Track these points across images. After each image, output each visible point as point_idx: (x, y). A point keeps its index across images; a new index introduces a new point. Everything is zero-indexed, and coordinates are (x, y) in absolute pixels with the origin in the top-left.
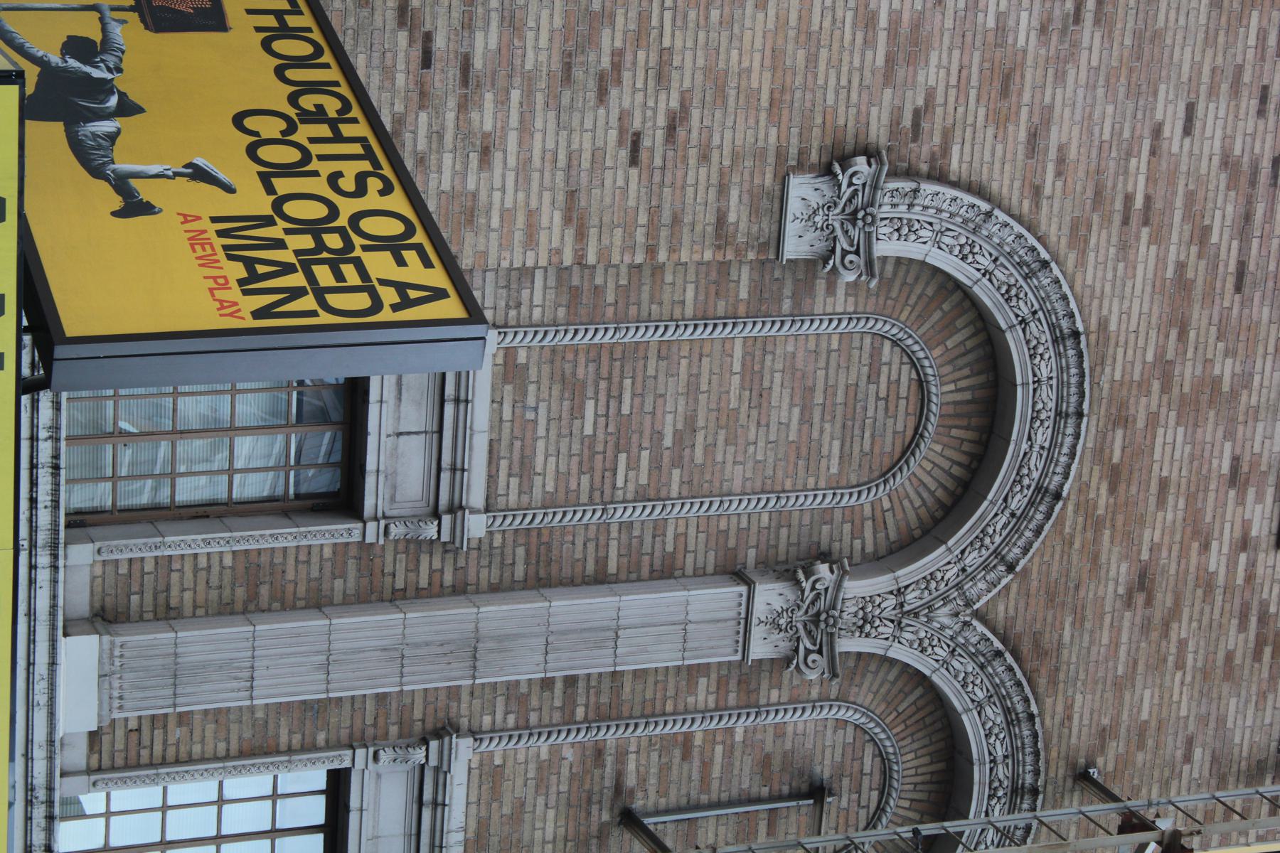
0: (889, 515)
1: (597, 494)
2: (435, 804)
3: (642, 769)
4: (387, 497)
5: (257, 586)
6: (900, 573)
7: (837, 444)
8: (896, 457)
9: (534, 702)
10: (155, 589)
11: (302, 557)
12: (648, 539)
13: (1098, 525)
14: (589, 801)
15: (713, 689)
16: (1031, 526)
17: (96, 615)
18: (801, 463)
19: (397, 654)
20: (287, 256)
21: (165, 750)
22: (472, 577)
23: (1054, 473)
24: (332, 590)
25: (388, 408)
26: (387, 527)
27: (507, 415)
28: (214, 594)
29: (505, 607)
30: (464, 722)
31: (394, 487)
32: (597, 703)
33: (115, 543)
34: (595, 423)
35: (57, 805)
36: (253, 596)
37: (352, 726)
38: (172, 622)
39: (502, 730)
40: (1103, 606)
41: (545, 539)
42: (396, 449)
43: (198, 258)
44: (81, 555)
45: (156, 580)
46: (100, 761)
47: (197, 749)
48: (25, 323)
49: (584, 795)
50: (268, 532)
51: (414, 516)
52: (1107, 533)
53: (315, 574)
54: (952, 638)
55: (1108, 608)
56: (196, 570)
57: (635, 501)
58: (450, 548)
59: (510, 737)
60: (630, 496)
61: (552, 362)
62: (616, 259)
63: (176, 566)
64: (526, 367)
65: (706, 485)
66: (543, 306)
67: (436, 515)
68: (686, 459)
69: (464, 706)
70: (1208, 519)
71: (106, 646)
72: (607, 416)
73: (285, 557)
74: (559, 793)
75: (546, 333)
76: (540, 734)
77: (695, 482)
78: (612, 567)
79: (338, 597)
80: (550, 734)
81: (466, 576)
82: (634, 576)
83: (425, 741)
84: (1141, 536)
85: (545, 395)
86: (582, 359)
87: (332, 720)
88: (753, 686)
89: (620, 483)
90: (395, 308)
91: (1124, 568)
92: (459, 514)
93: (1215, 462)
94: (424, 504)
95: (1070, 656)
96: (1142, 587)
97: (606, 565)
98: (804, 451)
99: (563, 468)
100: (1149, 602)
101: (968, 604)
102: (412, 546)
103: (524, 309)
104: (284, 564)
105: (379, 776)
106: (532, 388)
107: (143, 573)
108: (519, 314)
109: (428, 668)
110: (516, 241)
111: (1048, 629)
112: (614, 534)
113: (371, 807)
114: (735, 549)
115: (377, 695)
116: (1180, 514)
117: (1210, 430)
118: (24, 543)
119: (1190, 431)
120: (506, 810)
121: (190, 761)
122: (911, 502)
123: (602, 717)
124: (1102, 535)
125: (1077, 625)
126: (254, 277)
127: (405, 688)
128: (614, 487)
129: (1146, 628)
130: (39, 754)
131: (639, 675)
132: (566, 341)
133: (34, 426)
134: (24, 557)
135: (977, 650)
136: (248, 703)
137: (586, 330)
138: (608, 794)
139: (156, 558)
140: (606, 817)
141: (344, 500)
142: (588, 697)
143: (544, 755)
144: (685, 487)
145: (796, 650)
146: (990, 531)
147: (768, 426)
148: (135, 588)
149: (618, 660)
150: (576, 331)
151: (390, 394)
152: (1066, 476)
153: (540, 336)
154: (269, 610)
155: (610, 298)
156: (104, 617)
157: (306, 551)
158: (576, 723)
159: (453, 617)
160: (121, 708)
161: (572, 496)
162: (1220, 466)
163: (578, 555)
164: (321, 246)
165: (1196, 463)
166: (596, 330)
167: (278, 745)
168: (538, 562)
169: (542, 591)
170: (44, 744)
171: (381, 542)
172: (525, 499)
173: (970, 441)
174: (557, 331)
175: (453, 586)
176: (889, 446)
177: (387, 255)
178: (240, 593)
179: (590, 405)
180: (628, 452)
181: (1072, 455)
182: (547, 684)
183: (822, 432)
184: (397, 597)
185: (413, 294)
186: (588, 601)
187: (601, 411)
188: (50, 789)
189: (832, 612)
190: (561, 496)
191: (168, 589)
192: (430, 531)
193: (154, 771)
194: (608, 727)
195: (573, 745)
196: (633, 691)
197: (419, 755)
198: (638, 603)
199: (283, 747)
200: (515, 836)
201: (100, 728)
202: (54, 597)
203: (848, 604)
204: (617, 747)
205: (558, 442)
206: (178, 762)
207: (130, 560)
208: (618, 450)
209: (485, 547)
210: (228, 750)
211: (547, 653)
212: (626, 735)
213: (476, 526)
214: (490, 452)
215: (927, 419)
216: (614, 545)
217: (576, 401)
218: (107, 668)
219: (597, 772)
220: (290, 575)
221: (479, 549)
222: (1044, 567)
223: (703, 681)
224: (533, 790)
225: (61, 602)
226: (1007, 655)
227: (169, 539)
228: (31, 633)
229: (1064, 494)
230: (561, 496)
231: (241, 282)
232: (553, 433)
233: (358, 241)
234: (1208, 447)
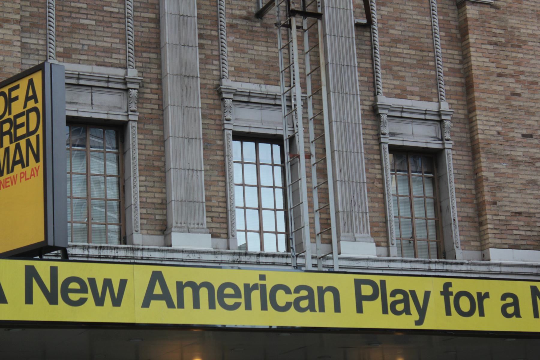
2: (249, 96)
3: (239, 8)
4: (119, 110)
5: (154, 166)
9: (209, 52)
10: (154, 209)
11: (143, 147)
14: (252, 31)
17: (163, 233)
19: (186, 109)
20: (12, 147)
21: (221, 207)
22: (155, 76)
24: (157, 135)
25: (81, 108)
26: (132, 111)
27: (85, 57)
28: (157, 185)
29: (168, 62)
30: (216, 82)
31: (115, 107)
32: (210, 26)
33: (133, 225)
34: (90, 19)
35: (241, 251)
36: (158, 168)
37: (215, 130)
38: (168, 202)
39: (220, 66)
41: (139, 44)
42: (98, 106)
43: (12, 185)
44: (138, 239)
45: (150, 208)
46: (224, 233)
47: (221, 194)
48: (38, 257)
49: (249, 33)
50: (132, 161)
51: (127, 99)
53: (150, 142)
56: (146, 192)
57: (125, 4)
58: (142, 85)
59: (223, 63)
60: (122, 6)
61: (63, 37)
62: (18, 6)
63: (144, 200)
64: (65, 48)
66: (38, 39)
67: (127, 90)
69: (209, 82)
72: (87, 14)
73: (142, 155)
74: (247, 44)
75: (50, 39)
76: (222, 51)
78: (153, 16)
79: (161, 133)
80: (222, 46)
81: (154, 79)
82: (157, 7)
83: (223, 99)
85: (77, 41)
86: (62, 24)
87: (212, 137)
89: (117, 10)
90: (36, 101)
92: (127, 80)
94: (122, 95)
97: (152, 18)
99: (109, 35)
102: (140, 101)
103: (39, 47)
104: (145, 155)
105: (236, 119)
106: (74, 46)
107: (147, 214)
108: (41, 50)
109: (192, 96)
110: (9, 49)
112: (139, 14)
113: (249, 123)
115: (202, 118)
118: (132, 261)
120: (253, 66)
121: (226, 197)
123: (216, 24)
126: (21, 161)
127: (200, 106)
128: (118, 13)
130: (219, 258)
131: (199, 8)
132: (54, 30)
133: (83, 256)
134: (136, 261)
136: (203, 172)
137: (49, 21)
138: (249, 23)
139: (140, 208)
140: (258, 24)
141: (119, 129)
142: (208, 29)
143: (231, 49)
148: (153, 217)
149: (193, 15)
150: (50, 25)
151: (75, 107)
153: (51, 42)
154: (165, 162)
155: (35, 10)
156: (164, 230)
157: (140, 146)
158: (218, 35)
159: (171, 85)
160: (202, 224)
161: (121, 31)
163: (147, 30)
164: (8, 132)
166: (49, 17)
167: (221, 161)
168: (149, 48)
169: (162, 46)
170: (215, 256)
171: (138, 114)
172: (122, 52)
174: (49, 34)
175: (158, 84)
177: (13, 104)
178: (157, 174)
179: (82, 21)
182: (201, 46)
184: (162, 108)
185: (31, 94)
186: (167, 27)
187: (85, 16)
191: (154, 203)
192: (134, 93)
193: (229, 212)
194: (221, 21)
195: (227, 37)
196: (206, 10)
197: (228, 102)
199: (222, 158)
200: (264, 63)
201: (210, 233)
202: (155, 250)
204: (229, 18)
205: (98, 36)
206: (226, 202)
207: (141, 218)
208: (102, 10)
209: (142, 70)
210: (222, 181)
211: (188, 46)
212: (224, 14)
213: (132, 73)
214: (101, 65)
216: (143, 15)
217: (80, 27)
218: (186, 229)
219: (239, 27)
220: (150, 152)
221: (142, 72)
224: (246, 55)
225: (157, 247)
227: (133, 202)
228: (169, 259)
230: (121, 36)
231: (23, 167)
232: (94, 38)
233: (7, 117)
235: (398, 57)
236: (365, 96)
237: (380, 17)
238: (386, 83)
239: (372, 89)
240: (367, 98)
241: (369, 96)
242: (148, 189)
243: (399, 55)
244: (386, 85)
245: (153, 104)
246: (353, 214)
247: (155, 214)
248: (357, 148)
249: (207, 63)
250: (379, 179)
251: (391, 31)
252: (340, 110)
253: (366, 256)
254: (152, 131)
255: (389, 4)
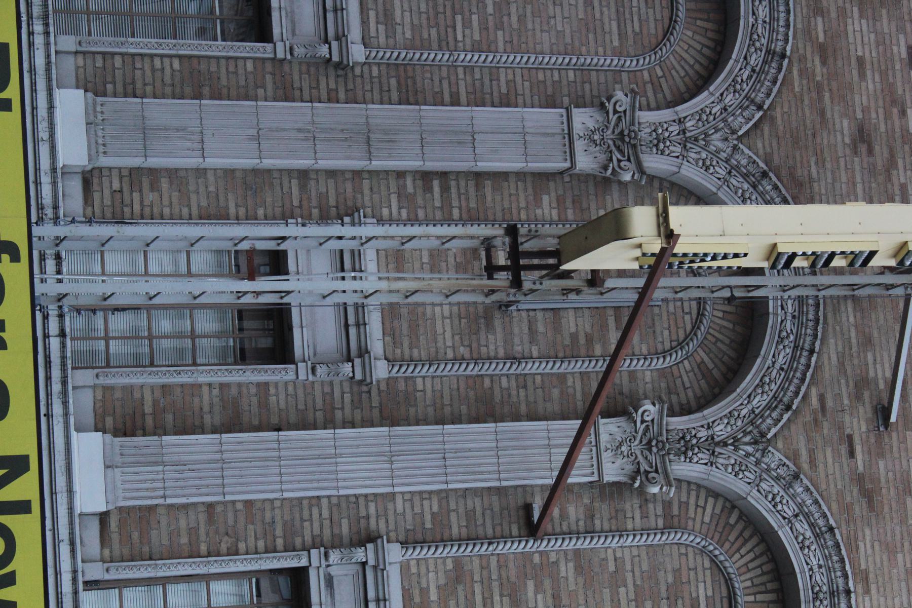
0: (663, 80)
1: (444, 44)
4: (289, 28)
6: (679, 108)
7: (614, 24)
8: (660, 38)
9: (420, 201)
12: (487, 81)
13: (819, 88)
15: (554, 205)
16: (768, 78)
18: (591, 36)
21: (142, 210)
23: (777, 40)
31: (293, 23)
32: (468, 206)
37: (283, 206)
40: (836, 151)
45: (124, 75)
47: (166, 211)
52: (827, 95)
53: (242, 83)
54: (727, 161)
55: (840, 154)
58: (342, 67)
65: (523, 45)
68: (506, 25)
69: (367, 198)
70: (900, 92)
71: (90, 101)
77: (515, 42)
84: (853, 100)
88: (585, 205)
89: (460, 38)
91: (845, 123)
93: (895, 48)
95: (820, 189)
96: (862, 140)
98: (591, 26)
100: (870, 152)
101: (734, 132)
102: (312, 69)
111: (799, 165)
112: (461, 76)
114: (552, 96)
116: (878, 86)
117: (885, 25)
118: (24, 18)
119: (871, 22)
122: (677, 72)
124: (823, 96)
125: (820, 165)
129: (872, 171)
130: (46, 179)
135: (748, 171)
142: (460, 201)
144: (508, 45)
145: (611, 160)
146: (739, 79)
147: (561, 5)
148: (109, 79)
152: (786, 41)
162: (900, 52)
165: (881, 48)
170: (49, 171)
171: (289, 57)
173: (712, 31)
176: (653, 29)
180: (462, 14)
181: (788, 26)
183: (602, 14)
188: (56, 207)
189: (632, 128)
190: (418, 43)
191: (134, 82)
196: (494, 199)
198: (485, 115)
203: (643, 126)
208: (454, 13)
213: (358, 53)
215: (677, 9)
216: (462, 84)
218: (92, 118)
220: (224, 82)
222: (786, 116)
223: (545, 198)
226: (771, 175)
228: (33, 84)
229: (788, 53)
234: (887, 37)
235: (484, 599)
236: (396, 523)
237: (553, 557)
238: (427, 569)
239: (411, 538)
240: (392, 526)
241: (396, 530)
242: (158, 74)
243: (489, 601)
244: (423, 570)
245: (310, 92)
246: (160, 468)
247: (114, 83)
248: (291, 482)
249: (399, 196)
250: (237, 546)
251: (531, 585)
252: (358, 446)
253: (77, 487)
254: (261, 87)
255: (581, 580)
